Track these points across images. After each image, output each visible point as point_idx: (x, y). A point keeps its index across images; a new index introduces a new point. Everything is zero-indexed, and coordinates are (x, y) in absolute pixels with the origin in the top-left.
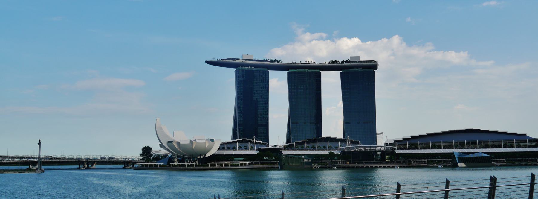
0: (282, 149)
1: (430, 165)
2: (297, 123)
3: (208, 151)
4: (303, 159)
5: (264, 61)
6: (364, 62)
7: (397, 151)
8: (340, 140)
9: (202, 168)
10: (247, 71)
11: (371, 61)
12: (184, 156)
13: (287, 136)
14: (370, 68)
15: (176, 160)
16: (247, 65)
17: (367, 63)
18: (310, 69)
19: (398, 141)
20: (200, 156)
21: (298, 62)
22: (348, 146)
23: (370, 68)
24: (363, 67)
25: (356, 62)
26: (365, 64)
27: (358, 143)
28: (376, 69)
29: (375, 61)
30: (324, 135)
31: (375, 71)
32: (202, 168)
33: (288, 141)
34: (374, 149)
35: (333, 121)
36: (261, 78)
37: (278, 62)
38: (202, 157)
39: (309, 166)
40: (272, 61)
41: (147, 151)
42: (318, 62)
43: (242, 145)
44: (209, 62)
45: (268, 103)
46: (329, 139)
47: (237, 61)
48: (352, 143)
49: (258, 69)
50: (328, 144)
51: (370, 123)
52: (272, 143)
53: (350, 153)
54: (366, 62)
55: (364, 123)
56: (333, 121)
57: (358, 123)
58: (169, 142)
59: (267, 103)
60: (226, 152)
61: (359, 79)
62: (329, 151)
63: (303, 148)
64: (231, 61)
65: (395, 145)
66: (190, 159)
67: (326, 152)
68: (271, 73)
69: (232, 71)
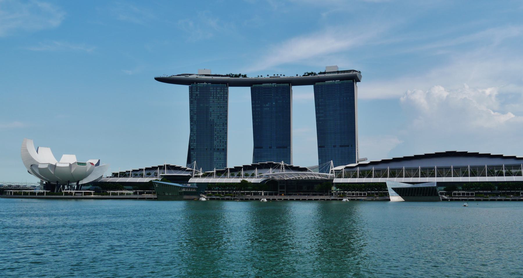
1: (370, 198)
2: (262, 148)
5: (227, 76)
6: (342, 72)
9: (49, 196)
14: (350, 79)
17: (346, 74)
21: (265, 77)
23: (350, 79)
26: (343, 74)
29: (354, 71)
32: (58, 196)
36: (219, 95)
37: (245, 76)
40: (236, 76)
42: (290, 74)
45: (226, 124)
47: (190, 77)
50: (256, 171)
51: (348, 146)
54: (344, 72)
55: (341, 146)
57: (334, 146)
59: (225, 124)
61: (336, 93)
62: (242, 179)
63: (225, 175)
64: (183, 77)
67: (238, 180)
68: (232, 90)
69: (186, 89)
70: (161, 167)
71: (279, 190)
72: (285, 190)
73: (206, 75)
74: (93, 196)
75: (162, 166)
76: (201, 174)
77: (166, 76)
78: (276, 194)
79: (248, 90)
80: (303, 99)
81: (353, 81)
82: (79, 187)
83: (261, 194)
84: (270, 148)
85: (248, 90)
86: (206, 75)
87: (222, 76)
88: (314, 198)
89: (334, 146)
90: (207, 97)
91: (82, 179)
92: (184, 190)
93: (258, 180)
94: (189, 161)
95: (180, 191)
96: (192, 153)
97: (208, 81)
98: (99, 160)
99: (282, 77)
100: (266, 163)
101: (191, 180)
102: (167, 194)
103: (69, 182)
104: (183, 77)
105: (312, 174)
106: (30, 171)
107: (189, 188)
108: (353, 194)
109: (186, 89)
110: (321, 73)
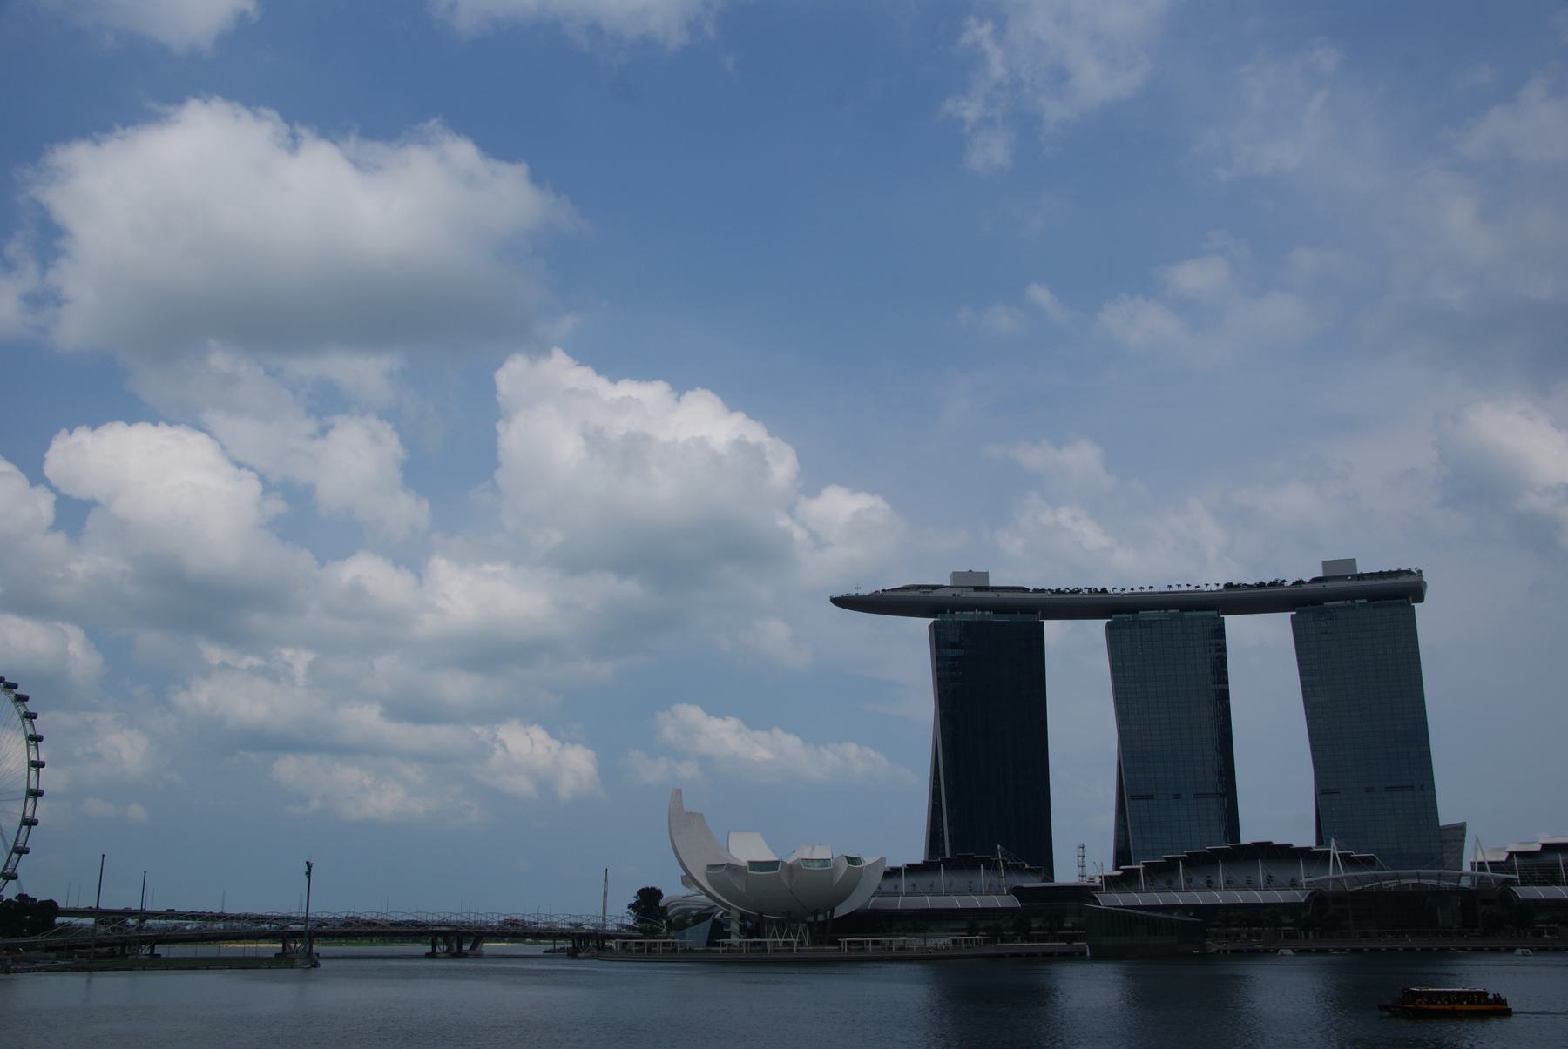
0: (1096, 888)
2: (1149, 797)
3: (842, 899)
8: (1304, 853)
10: (969, 624)
11: (1399, 573)
12: (761, 914)
13: (1117, 841)
15: (735, 926)
19: (1520, 854)
20: (816, 913)
22: (1334, 875)
25: (1344, 577)
27: (1370, 863)
28: (1420, 599)
29: (1409, 572)
30: (1247, 838)
31: (1416, 606)
33: (1122, 856)
34: (1434, 882)
35: (1276, 791)
38: (821, 918)
41: (648, 900)
43: (960, 880)
44: (842, 602)
46: (1265, 851)
47: (936, 593)
48: (1348, 860)
49: (1006, 618)
50: (1261, 871)
51: (1411, 788)
52: (1065, 873)
53: (1340, 898)
54: (1381, 574)
55: (1390, 789)
56: (1276, 791)
58: (711, 867)
60: (901, 903)
63: (1171, 886)
65: (1511, 870)
66: (781, 924)
79: (1097, 628)
80: (1261, 652)
84: (1177, 796)
85: (1097, 628)
93: (1299, 896)
99: (1192, 588)
109: (923, 624)
110: (1300, 582)
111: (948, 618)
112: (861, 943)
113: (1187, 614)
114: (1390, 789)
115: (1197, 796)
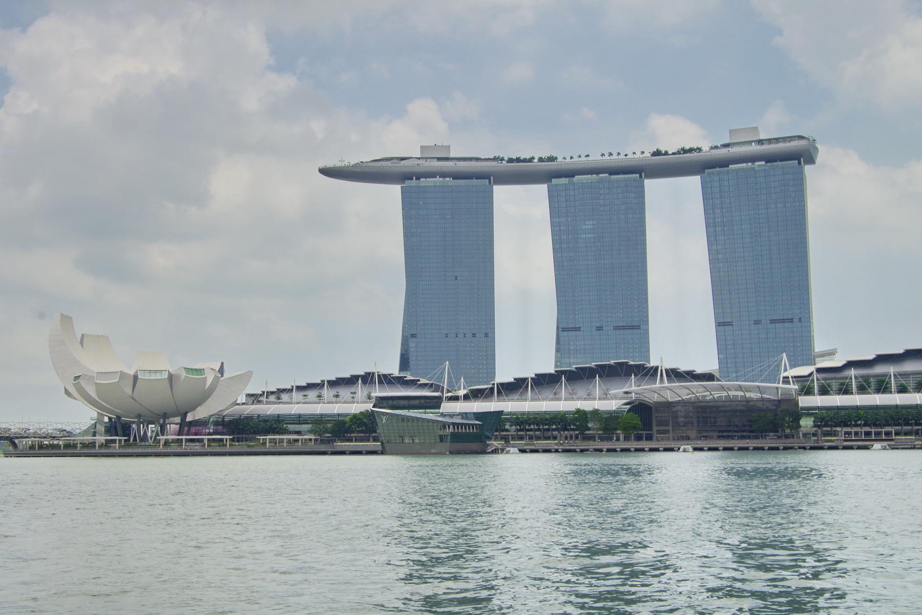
2: (577, 329)
4: (444, 425)
6: (770, 141)
7: (804, 401)
11: (791, 138)
16: (432, 175)
18: (610, 174)
19: (819, 370)
24: (770, 159)
29: (801, 138)
39: (475, 446)
40: (510, 161)
42: (637, 150)
50: (597, 386)
51: (791, 321)
54: (777, 140)
55: (773, 321)
57: (757, 322)
70: (367, 379)
71: (655, 428)
72: (670, 428)
73: (439, 159)
74: (228, 449)
75: (368, 374)
76: (462, 392)
77: (346, 163)
78: (649, 438)
81: (799, 163)
82: (186, 427)
83: (618, 439)
86: (439, 159)
87: (478, 159)
88: (721, 444)
89: (757, 322)
90: (445, 210)
91: (193, 408)
92: (451, 430)
94: (404, 364)
95: (441, 433)
96: (412, 345)
97: (444, 175)
98: (222, 363)
99: (622, 156)
100: (612, 362)
101: (447, 407)
102: (407, 440)
103: (165, 416)
104: (388, 163)
105: (723, 388)
106: (72, 390)
107: (458, 424)
108: (849, 433)
109: (395, 190)
111: (414, 182)
112: (222, 440)
113: (613, 177)
114: (773, 321)
115: (616, 328)
